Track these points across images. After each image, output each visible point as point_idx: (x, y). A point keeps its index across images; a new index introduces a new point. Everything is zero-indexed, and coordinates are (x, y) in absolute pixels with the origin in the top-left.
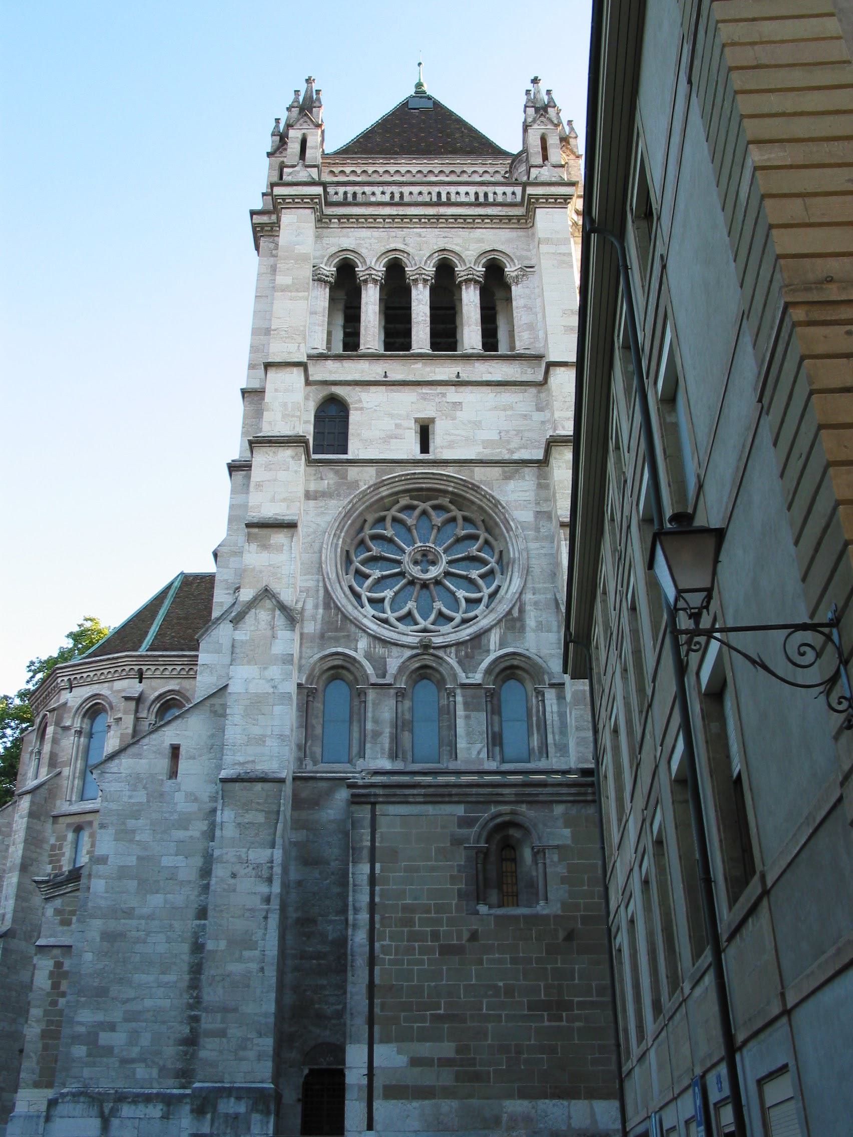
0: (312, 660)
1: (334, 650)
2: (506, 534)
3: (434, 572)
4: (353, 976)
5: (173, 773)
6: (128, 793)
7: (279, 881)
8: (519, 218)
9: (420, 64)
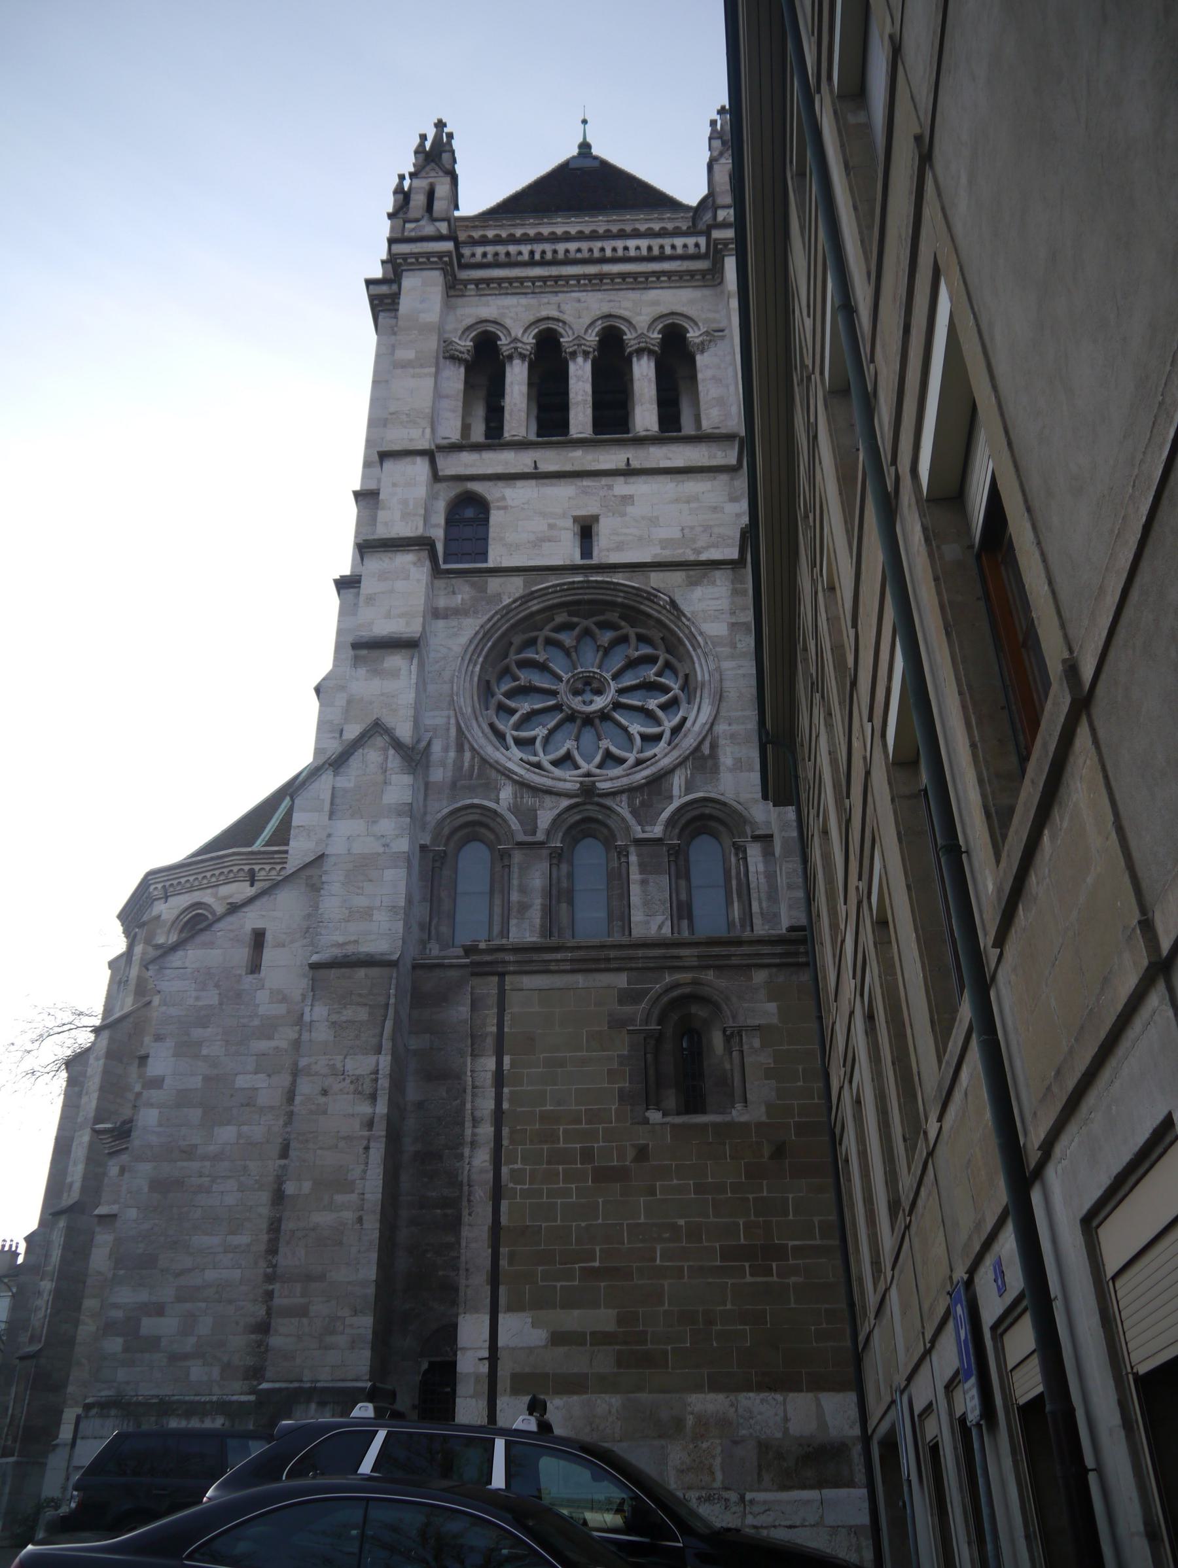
0: (439, 816)
1: (468, 802)
2: (693, 653)
3: (600, 703)
4: (470, 1214)
5: (255, 967)
6: (194, 994)
7: (387, 1097)
8: (704, 273)
9: (585, 122)
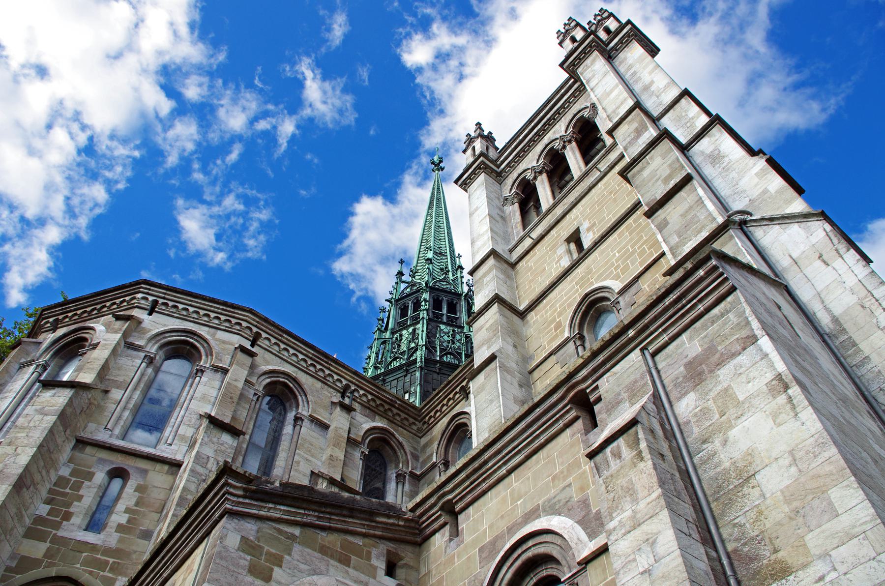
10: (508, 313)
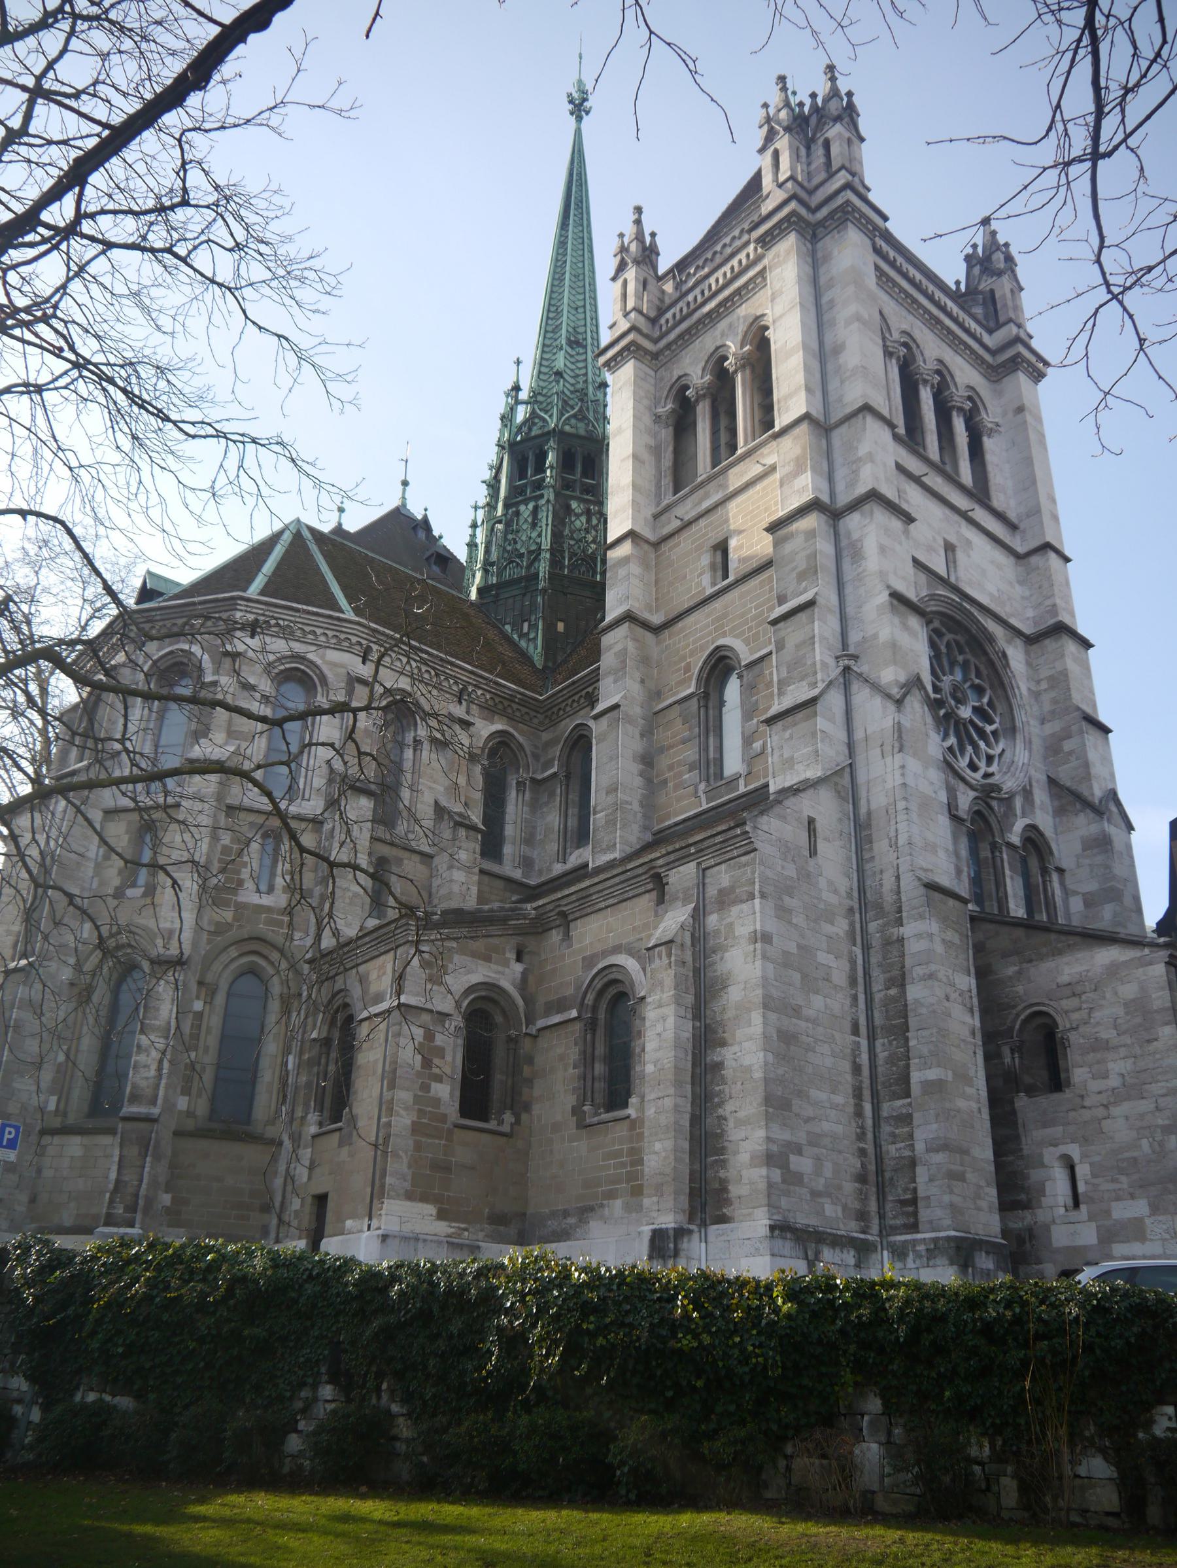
5: (813, 852)
10: (640, 631)
